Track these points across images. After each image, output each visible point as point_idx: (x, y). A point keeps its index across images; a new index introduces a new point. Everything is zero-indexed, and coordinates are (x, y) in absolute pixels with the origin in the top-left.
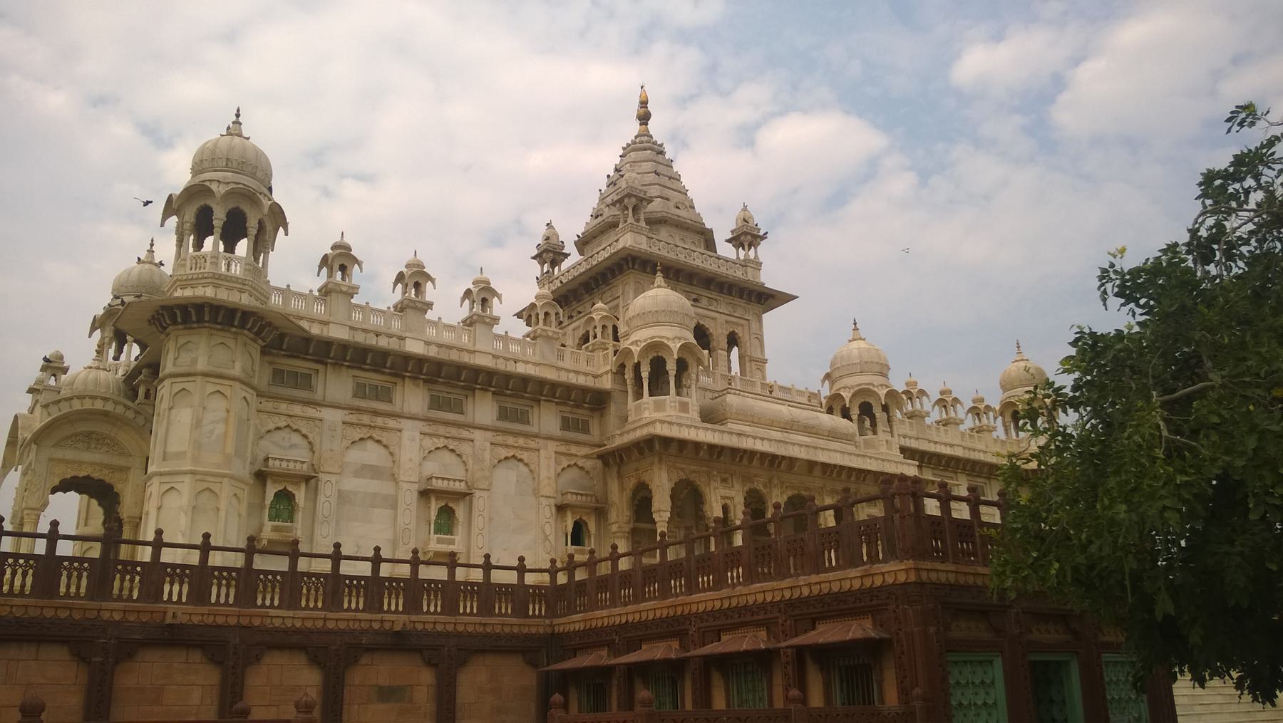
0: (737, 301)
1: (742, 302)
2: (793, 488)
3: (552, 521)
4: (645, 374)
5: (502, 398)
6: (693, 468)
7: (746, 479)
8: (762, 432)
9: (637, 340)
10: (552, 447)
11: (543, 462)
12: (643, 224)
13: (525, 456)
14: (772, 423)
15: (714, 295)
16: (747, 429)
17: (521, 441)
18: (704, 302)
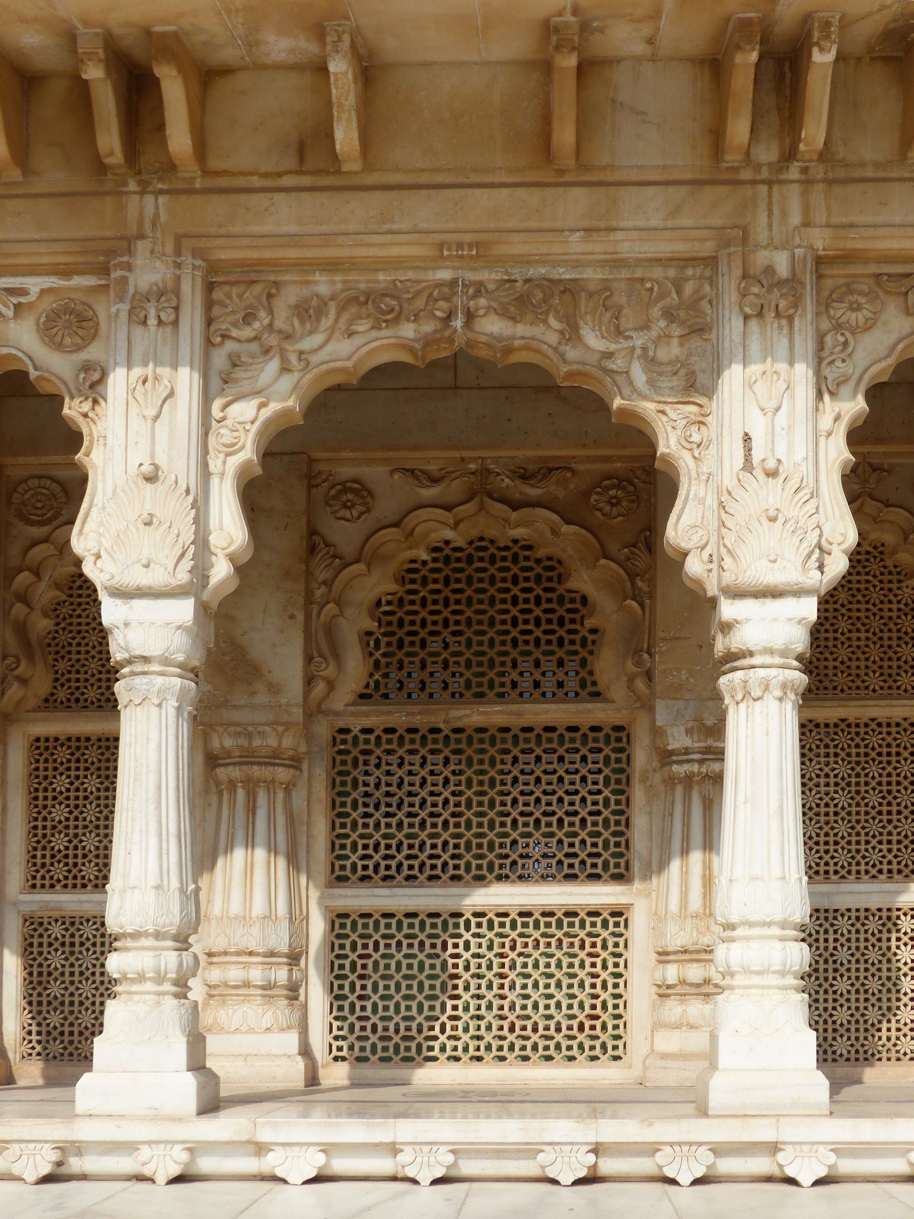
2: (383, 306)
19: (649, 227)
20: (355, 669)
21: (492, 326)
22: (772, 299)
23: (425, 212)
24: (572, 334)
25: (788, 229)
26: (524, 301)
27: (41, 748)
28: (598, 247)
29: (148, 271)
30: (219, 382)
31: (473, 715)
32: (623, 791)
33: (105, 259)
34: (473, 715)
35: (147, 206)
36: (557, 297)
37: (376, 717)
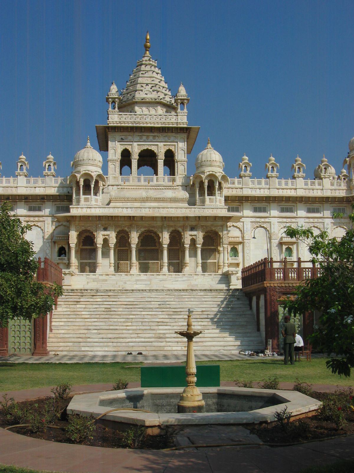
0: (170, 134)
1: (174, 134)
2: (145, 227)
3: (50, 248)
4: (81, 186)
5: (28, 203)
6: (88, 225)
7: (116, 226)
8: (129, 205)
11: (46, 225)
12: (117, 109)
13: (39, 224)
14: (135, 200)
15: (156, 134)
17: (37, 219)
18: (151, 138)
19: (159, 223)
20: (140, 244)
21: (151, 229)
22: (165, 228)
23: (147, 222)
24: (155, 229)
25: (166, 223)
26: (152, 228)
28: (156, 225)
30: (137, 232)
33: (131, 225)
35: (134, 222)
36: (153, 227)
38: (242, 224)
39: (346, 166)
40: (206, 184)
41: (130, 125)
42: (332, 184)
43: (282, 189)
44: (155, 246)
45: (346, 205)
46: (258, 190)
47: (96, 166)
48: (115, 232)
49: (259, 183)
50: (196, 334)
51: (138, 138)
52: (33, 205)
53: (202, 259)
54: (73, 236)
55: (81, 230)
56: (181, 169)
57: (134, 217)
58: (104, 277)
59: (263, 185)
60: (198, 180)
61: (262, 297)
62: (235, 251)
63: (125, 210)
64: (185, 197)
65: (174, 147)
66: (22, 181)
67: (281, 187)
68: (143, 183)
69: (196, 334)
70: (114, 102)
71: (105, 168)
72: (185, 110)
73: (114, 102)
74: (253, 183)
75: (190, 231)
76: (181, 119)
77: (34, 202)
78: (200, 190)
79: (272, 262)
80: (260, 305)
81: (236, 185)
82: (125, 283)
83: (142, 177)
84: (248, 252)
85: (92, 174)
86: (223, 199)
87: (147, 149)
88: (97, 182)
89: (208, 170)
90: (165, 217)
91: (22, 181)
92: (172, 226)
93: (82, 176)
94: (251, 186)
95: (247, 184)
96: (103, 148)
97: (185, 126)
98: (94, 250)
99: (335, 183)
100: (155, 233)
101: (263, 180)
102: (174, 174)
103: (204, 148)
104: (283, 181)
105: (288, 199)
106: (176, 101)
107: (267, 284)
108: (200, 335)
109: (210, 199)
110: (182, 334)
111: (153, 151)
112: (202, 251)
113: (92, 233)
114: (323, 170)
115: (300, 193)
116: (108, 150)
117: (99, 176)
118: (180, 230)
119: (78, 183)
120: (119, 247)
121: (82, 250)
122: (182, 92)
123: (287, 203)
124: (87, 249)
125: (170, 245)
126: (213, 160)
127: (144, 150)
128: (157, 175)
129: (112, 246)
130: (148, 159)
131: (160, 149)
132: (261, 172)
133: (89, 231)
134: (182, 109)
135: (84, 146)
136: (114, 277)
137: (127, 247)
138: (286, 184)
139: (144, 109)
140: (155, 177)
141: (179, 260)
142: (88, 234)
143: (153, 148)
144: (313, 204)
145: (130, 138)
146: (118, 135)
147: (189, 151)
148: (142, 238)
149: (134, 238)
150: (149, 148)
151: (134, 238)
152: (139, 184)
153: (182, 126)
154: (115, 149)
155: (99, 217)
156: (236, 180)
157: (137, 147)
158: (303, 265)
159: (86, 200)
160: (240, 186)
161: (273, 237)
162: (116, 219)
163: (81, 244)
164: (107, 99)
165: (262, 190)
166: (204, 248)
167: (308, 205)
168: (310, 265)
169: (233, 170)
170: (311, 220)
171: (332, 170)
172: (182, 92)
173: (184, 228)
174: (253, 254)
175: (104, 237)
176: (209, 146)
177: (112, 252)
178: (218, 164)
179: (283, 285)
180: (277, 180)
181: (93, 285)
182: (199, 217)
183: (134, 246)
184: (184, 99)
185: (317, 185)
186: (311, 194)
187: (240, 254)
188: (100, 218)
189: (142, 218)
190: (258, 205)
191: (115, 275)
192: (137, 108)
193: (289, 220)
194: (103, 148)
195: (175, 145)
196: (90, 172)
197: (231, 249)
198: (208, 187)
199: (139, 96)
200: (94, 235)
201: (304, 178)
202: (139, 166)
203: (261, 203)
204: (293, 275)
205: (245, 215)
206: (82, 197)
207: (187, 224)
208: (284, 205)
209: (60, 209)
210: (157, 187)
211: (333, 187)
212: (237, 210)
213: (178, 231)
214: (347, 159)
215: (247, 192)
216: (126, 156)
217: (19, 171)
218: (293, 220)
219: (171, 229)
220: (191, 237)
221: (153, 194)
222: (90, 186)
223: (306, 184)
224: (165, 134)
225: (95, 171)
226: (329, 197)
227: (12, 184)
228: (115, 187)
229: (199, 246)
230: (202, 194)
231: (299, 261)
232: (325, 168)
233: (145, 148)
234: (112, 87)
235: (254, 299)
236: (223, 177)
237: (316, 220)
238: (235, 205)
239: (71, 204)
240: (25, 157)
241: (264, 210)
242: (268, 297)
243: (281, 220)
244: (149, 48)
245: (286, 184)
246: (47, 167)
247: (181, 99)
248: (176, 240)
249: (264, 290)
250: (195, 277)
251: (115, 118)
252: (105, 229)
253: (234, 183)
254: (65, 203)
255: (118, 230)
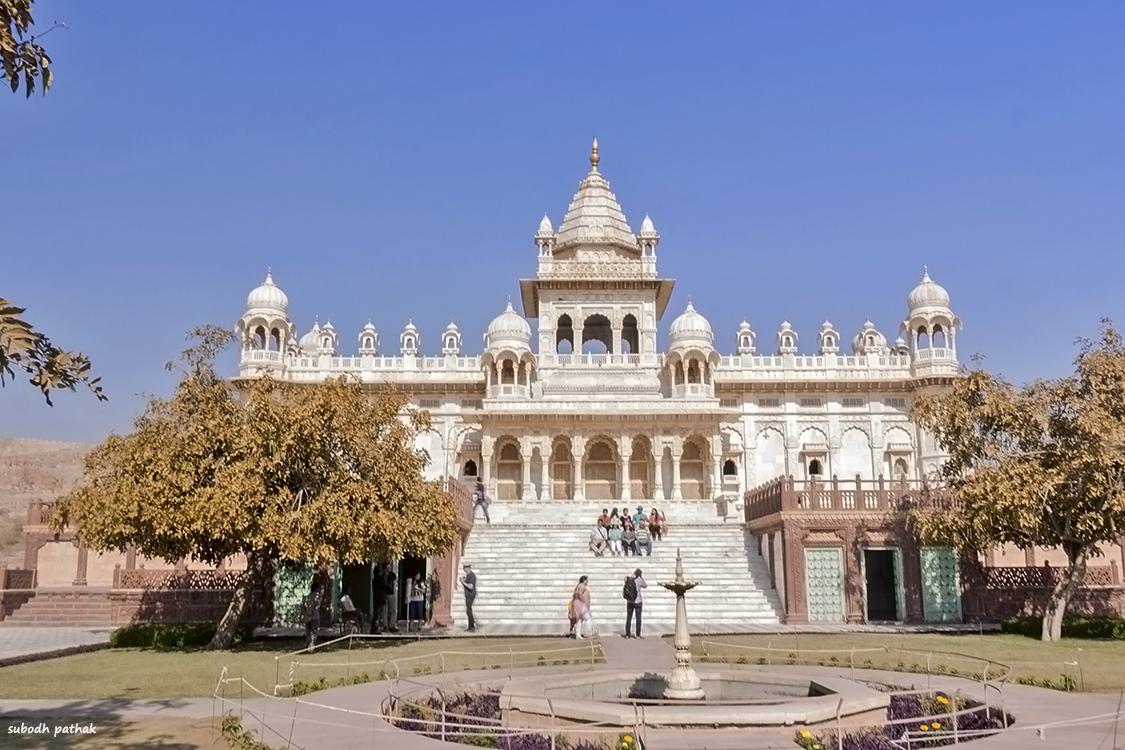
0: (630, 291)
2: (595, 431)
6: (511, 427)
8: (571, 397)
9: (497, 348)
10: (453, 420)
14: (580, 390)
15: (609, 292)
16: (558, 397)
18: (602, 297)
20: (588, 456)
21: (604, 433)
22: (625, 431)
26: (606, 431)
27: (555, 466)
29: (577, 428)
30: (583, 437)
31: (602, 462)
32: (615, 469)
33: (574, 427)
34: (599, 462)
36: (610, 431)
37: (591, 462)
38: (742, 424)
39: (904, 333)
40: (686, 369)
41: (572, 278)
42: (882, 362)
43: (803, 371)
44: (610, 459)
45: (905, 393)
46: (765, 374)
47: (522, 340)
48: (630, 438)
49: (767, 363)
50: (689, 587)
51: (584, 298)
52: (427, 398)
53: (682, 477)
54: (488, 443)
55: (499, 436)
56: (647, 342)
57: (578, 416)
58: (534, 506)
59: (773, 365)
60: (675, 360)
61: (778, 536)
62: (729, 468)
63: (565, 406)
64: (654, 384)
65: (636, 310)
66: (409, 362)
67: (801, 368)
68: (590, 364)
69: (689, 587)
70: (546, 244)
71: (534, 341)
72: (653, 255)
73: (546, 244)
74: (757, 363)
75: (663, 435)
76: (648, 268)
77: (432, 393)
78: (677, 375)
79: (791, 482)
80: (775, 549)
81: (732, 366)
82: (567, 515)
83: (590, 356)
84: (751, 466)
85: (516, 352)
86: (713, 386)
87: (597, 315)
88: (522, 365)
89: (688, 345)
90: (626, 416)
91: (409, 362)
92: (636, 430)
93: (500, 356)
94: (754, 368)
95: (748, 365)
96: (531, 312)
97: (654, 279)
98: (519, 466)
99: (887, 361)
100: (611, 440)
101: (773, 358)
102: (637, 352)
103: (681, 311)
104: (804, 359)
105: (812, 387)
106: (639, 241)
107: (785, 515)
108: (696, 588)
109: (692, 388)
110: (668, 587)
111: (606, 318)
112: (682, 466)
113: (516, 440)
114: (868, 341)
115: (832, 376)
116: (537, 316)
117: (526, 355)
118: (648, 434)
119: (494, 366)
120: (556, 460)
121: (500, 465)
122: (648, 227)
123: (811, 394)
124: (507, 464)
125: (633, 457)
126: (693, 328)
127: (592, 316)
128: (611, 352)
129: (546, 459)
130: (597, 328)
131: (615, 312)
132: (768, 346)
133: (511, 438)
134: (648, 253)
135: (501, 311)
136: (548, 506)
137: (567, 460)
138: (809, 363)
139: (591, 253)
140: (609, 356)
141: (646, 479)
142: (510, 441)
143: (604, 313)
144: (853, 393)
145: (571, 297)
146: (553, 293)
147: (659, 316)
148: (590, 447)
149: (579, 447)
150: (600, 313)
151: (579, 447)
152: (584, 366)
153: (649, 279)
154: (549, 313)
155: (527, 416)
156: (731, 358)
157: (581, 310)
158: (842, 487)
159: (508, 391)
160: (739, 368)
161: (791, 444)
162: (553, 419)
163: (500, 457)
164: (536, 240)
165: (771, 373)
166: (686, 461)
167: (844, 394)
168: (853, 486)
169: (726, 343)
170: (851, 418)
171: (881, 340)
172: (648, 227)
173: (654, 431)
174: (761, 468)
175: (534, 446)
176: (690, 307)
177: (546, 469)
178: (704, 334)
179: (811, 517)
180: (795, 358)
181: (519, 519)
182: (677, 416)
183: (578, 459)
184: (651, 239)
185: (857, 363)
186: (850, 377)
187: (740, 471)
188: (526, 418)
189: (590, 417)
190: (765, 396)
191: (550, 503)
192: (580, 253)
193: (815, 418)
194: (531, 312)
195: (637, 308)
196: (512, 350)
197: (897, 461)
198: (690, 369)
199: (582, 235)
200: (519, 443)
201: (837, 354)
202: (585, 340)
203: (770, 394)
204: (825, 502)
205: (746, 411)
206: (501, 386)
207: (659, 427)
208: (806, 395)
209: (465, 404)
210: (611, 372)
211: (884, 367)
212: (734, 404)
213: (645, 437)
214: (906, 323)
215: (748, 376)
216: (565, 323)
217: (405, 348)
218: (822, 418)
219: (634, 434)
220: (665, 445)
221: (608, 382)
222: (510, 369)
223: (840, 363)
224: (624, 291)
225: (518, 347)
226: (877, 383)
227: (394, 367)
228: (550, 372)
229: (677, 459)
230: (680, 380)
231: (835, 481)
232: (871, 338)
233: (594, 313)
234: (543, 222)
235: (765, 538)
236: (713, 356)
237: (858, 418)
238: (731, 396)
239: (485, 397)
240: (414, 327)
241: (776, 404)
242: (787, 537)
243: (802, 418)
244: (597, 162)
245: (809, 363)
246: (448, 342)
247: (646, 239)
248: (642, 449)
249: (781, 525)
250: (672, 505)
251: (547, 268)
252: (537, 433)
253: (727, 363)
254: (474, 397)
255: (554, 436)
